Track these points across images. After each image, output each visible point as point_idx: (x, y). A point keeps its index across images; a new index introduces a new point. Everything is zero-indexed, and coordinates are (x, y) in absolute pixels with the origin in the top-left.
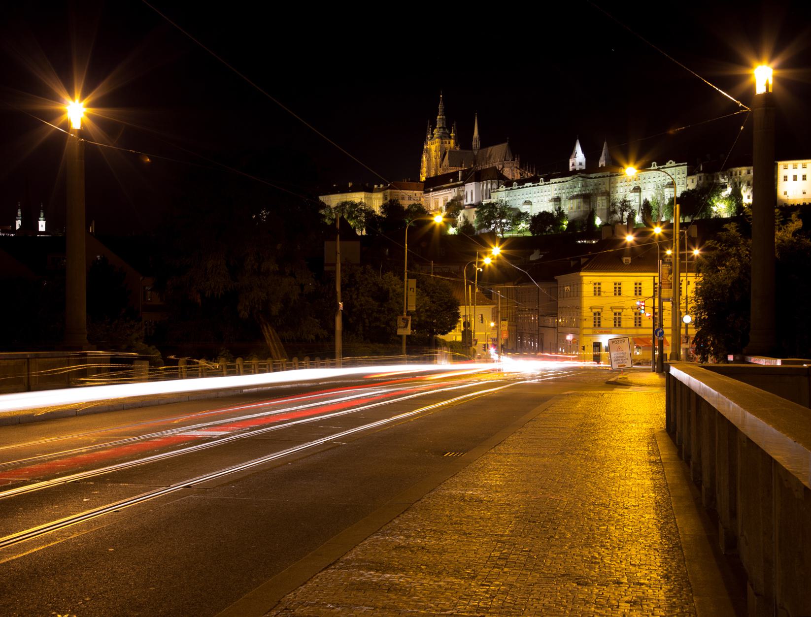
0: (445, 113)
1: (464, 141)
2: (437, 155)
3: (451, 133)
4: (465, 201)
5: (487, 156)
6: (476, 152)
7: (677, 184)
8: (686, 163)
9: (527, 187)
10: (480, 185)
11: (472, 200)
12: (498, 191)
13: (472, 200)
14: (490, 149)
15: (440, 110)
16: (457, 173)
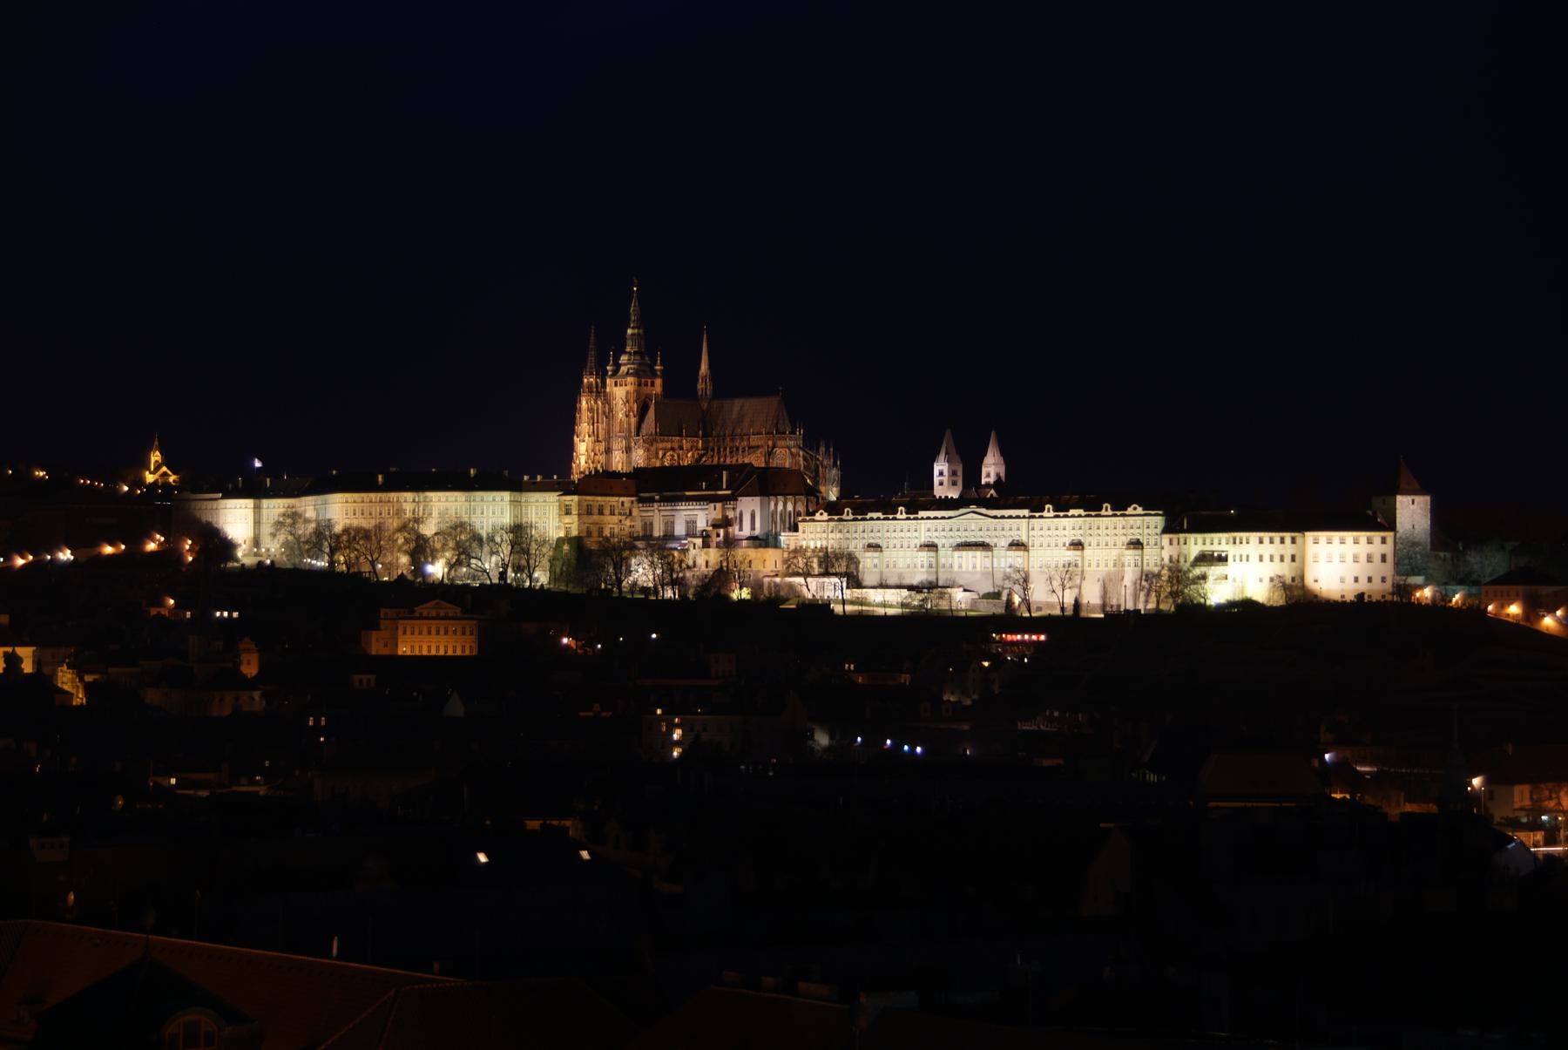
0: (642, 323)
1: (679, 384)
2: (631, 409)
3: (655, 364)
4: (737, 528)
5: (734, 417)
6: (706, 405)
7: (1145, 544)
8: (1160, 512)
9: (872, 519)
10: (769, 503)
11: (753, 528)
12: (814, 521)
13: (753, 528)
14: (737, 403)
15: (633, 318)
16: (719, 468)
